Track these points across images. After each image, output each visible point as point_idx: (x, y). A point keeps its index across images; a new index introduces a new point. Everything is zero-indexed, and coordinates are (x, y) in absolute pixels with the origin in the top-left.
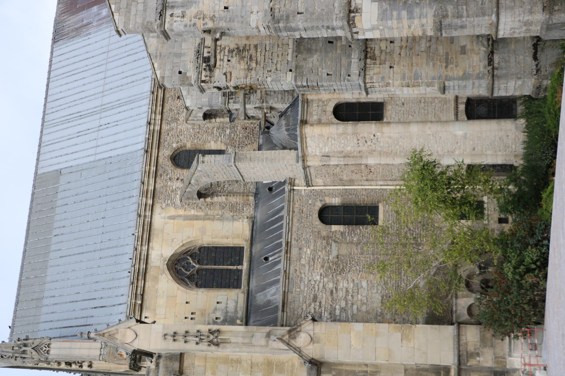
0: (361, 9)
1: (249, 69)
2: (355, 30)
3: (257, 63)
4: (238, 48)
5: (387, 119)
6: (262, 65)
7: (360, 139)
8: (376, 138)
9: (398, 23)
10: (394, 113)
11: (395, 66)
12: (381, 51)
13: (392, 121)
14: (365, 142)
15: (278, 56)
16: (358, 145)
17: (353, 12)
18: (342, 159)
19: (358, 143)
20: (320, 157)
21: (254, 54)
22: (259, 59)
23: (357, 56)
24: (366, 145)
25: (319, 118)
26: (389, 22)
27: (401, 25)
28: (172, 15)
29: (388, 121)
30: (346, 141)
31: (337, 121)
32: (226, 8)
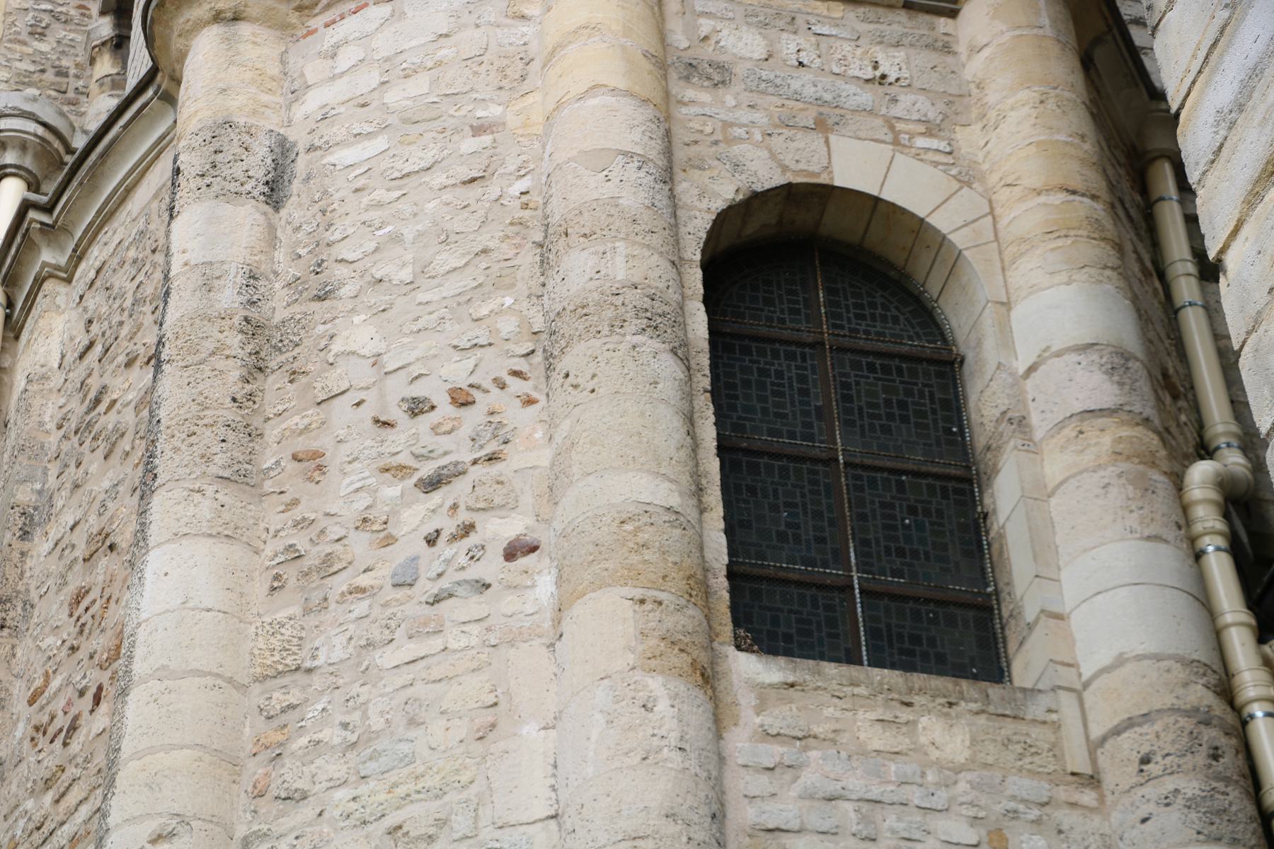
5: (765, 695)
7: (473, 418)
8: (492, 567)
10: (856, 783)
13: (739, 743)
14: (427, 469)
16: (396, 413)
18: (228, 297)
19: (417, 408)
20: (272, 121)
24: (392, 491)
25: (740, 70)
29: (746, 700)
30: (453, 286)
31: (697, 226)
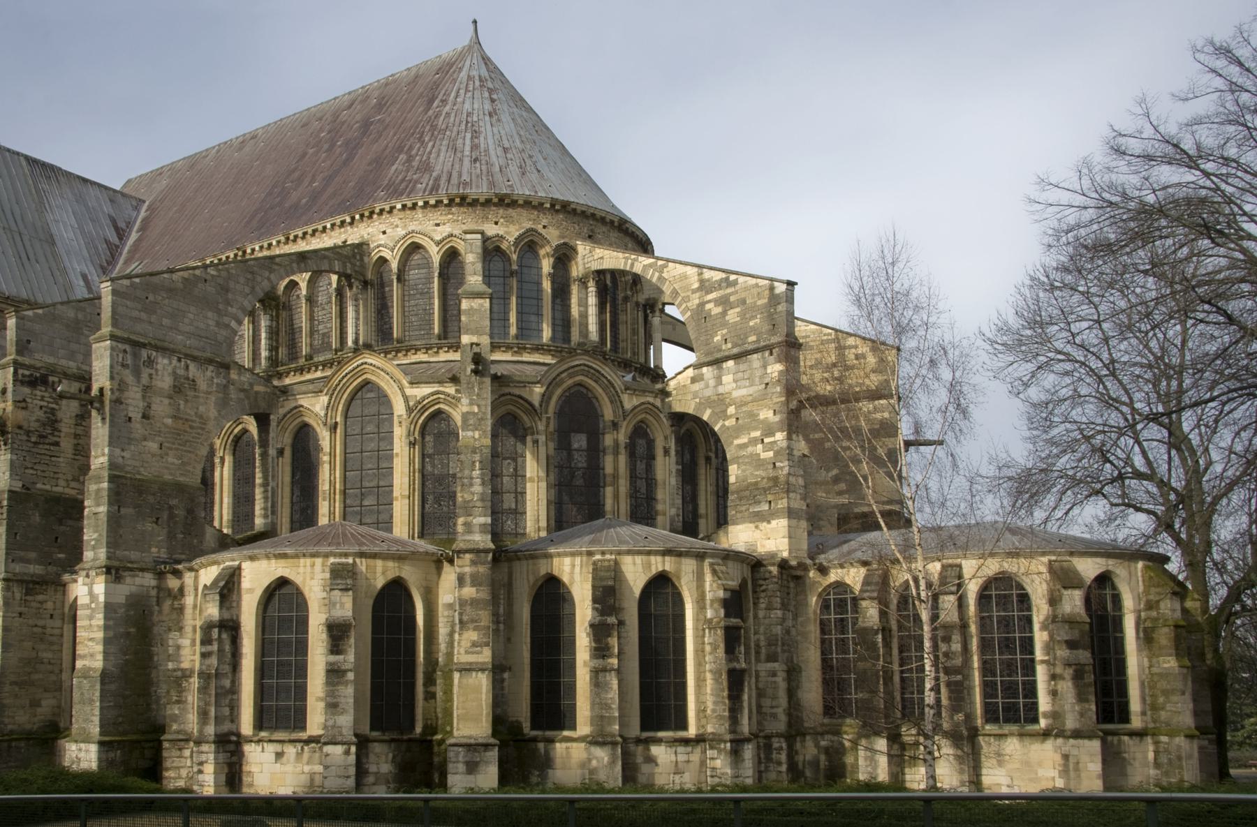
0: (119, 582)
1: (28, 433)
2: (93, 573)
3: (35, 443)
4: (56, 421)
6: (33, 450)
9: (98, 626)
11: (21, 619)
12: (41, 603)
15: (44, 471)
17: (117, 573)
21: (47, 441)
22: (41, 446)
23: (37, 572)
26: (101, 616)
27: (95, 629)
28: (125, 351)
32: (130, 418)
